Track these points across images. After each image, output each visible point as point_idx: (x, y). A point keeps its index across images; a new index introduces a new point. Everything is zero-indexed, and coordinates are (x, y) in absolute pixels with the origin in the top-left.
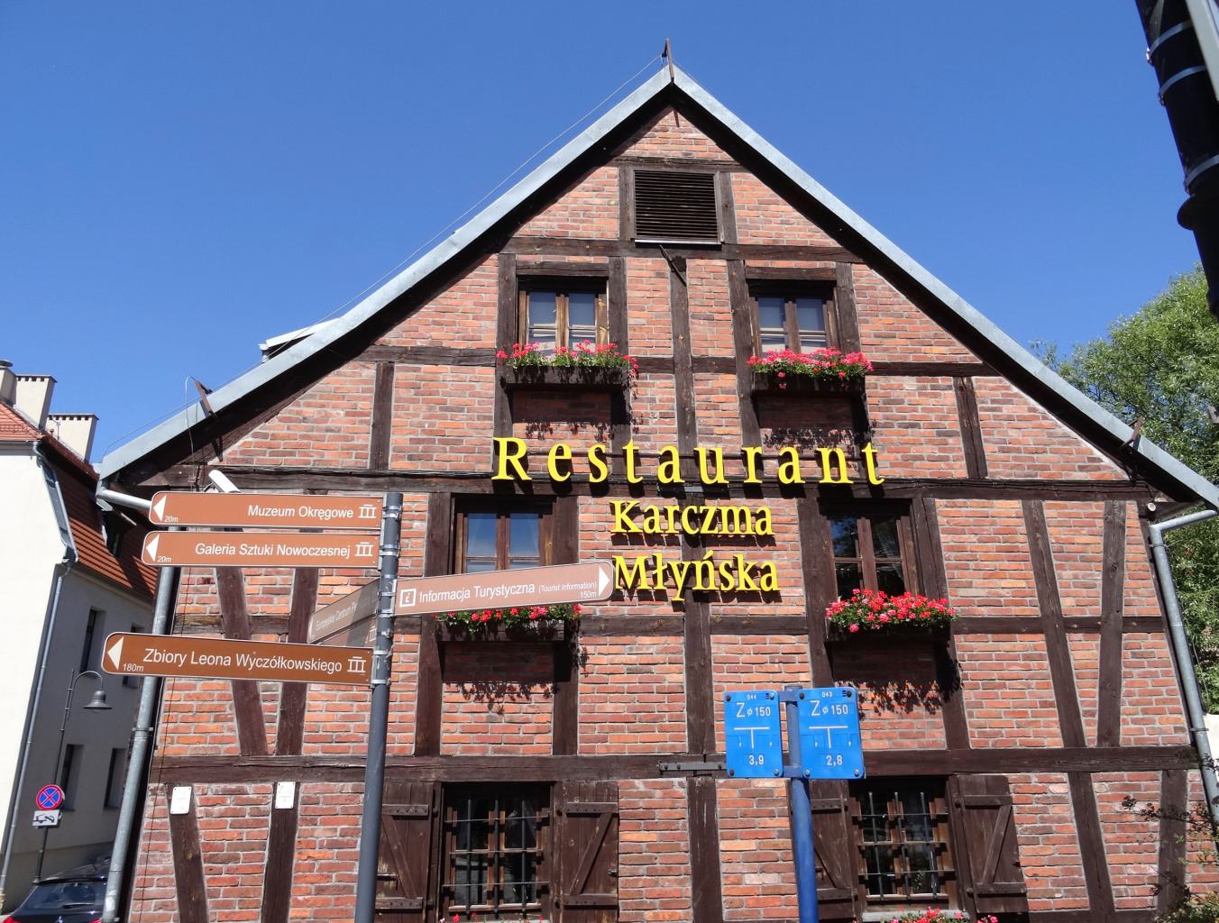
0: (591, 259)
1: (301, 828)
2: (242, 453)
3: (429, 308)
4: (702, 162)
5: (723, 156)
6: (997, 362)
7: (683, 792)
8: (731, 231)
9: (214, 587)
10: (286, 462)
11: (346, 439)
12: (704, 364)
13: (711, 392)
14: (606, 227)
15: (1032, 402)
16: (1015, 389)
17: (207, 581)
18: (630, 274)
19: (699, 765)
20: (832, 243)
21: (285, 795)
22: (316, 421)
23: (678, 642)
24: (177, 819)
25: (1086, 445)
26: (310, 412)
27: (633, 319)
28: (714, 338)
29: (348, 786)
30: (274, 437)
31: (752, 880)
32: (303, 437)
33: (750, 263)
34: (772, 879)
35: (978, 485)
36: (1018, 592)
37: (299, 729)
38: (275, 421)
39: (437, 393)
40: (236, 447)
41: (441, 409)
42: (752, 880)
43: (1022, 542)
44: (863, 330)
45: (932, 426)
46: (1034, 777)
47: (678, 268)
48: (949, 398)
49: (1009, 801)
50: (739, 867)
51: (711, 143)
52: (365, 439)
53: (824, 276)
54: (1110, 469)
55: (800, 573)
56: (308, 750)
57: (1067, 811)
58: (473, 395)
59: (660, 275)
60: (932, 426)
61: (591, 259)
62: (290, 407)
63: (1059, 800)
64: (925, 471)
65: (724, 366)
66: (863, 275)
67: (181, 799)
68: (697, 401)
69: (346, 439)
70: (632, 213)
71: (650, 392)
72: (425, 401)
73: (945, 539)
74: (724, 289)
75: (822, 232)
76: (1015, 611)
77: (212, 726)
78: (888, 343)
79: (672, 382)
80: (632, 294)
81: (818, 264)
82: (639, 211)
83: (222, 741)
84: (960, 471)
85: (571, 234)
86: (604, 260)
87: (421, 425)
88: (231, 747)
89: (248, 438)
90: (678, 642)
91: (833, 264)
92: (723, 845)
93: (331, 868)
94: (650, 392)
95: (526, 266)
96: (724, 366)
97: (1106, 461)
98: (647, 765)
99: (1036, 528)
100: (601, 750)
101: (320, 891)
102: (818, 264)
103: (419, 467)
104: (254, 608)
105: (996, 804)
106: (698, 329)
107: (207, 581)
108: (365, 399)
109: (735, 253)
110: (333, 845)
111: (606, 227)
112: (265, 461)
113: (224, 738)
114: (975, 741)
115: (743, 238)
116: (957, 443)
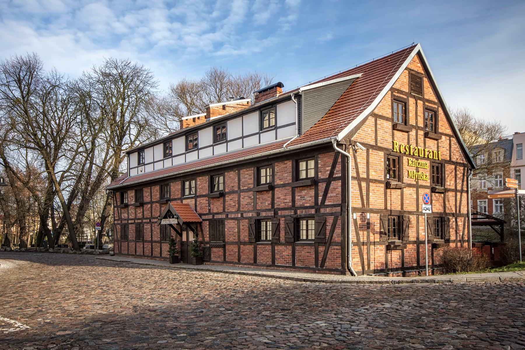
2: (356, 137)
10: (362, 141)
13: (420, 135)
17: (354, 169)
19: (417, 213)
20: (436, 101)
22: (367, 131)
30: (361, 134)
32: (365, 135)
35: (450, 162)
38: (360, 130)
39: (383, 127)
41: (385, 132)
45: (446, 148)
47: (416, 103)
56: (371, 207)
58: (389, 129)
60: (446, 148)
66: (440, 111)
72: (382, 129)
83: (359, 204)
86: (405, 97)
87: (382, 135)
104: (361, 176)
106: (419, 118)
107: (354, 169)
108: (373, 127)
109: (423, 100)
115: (426, 97)
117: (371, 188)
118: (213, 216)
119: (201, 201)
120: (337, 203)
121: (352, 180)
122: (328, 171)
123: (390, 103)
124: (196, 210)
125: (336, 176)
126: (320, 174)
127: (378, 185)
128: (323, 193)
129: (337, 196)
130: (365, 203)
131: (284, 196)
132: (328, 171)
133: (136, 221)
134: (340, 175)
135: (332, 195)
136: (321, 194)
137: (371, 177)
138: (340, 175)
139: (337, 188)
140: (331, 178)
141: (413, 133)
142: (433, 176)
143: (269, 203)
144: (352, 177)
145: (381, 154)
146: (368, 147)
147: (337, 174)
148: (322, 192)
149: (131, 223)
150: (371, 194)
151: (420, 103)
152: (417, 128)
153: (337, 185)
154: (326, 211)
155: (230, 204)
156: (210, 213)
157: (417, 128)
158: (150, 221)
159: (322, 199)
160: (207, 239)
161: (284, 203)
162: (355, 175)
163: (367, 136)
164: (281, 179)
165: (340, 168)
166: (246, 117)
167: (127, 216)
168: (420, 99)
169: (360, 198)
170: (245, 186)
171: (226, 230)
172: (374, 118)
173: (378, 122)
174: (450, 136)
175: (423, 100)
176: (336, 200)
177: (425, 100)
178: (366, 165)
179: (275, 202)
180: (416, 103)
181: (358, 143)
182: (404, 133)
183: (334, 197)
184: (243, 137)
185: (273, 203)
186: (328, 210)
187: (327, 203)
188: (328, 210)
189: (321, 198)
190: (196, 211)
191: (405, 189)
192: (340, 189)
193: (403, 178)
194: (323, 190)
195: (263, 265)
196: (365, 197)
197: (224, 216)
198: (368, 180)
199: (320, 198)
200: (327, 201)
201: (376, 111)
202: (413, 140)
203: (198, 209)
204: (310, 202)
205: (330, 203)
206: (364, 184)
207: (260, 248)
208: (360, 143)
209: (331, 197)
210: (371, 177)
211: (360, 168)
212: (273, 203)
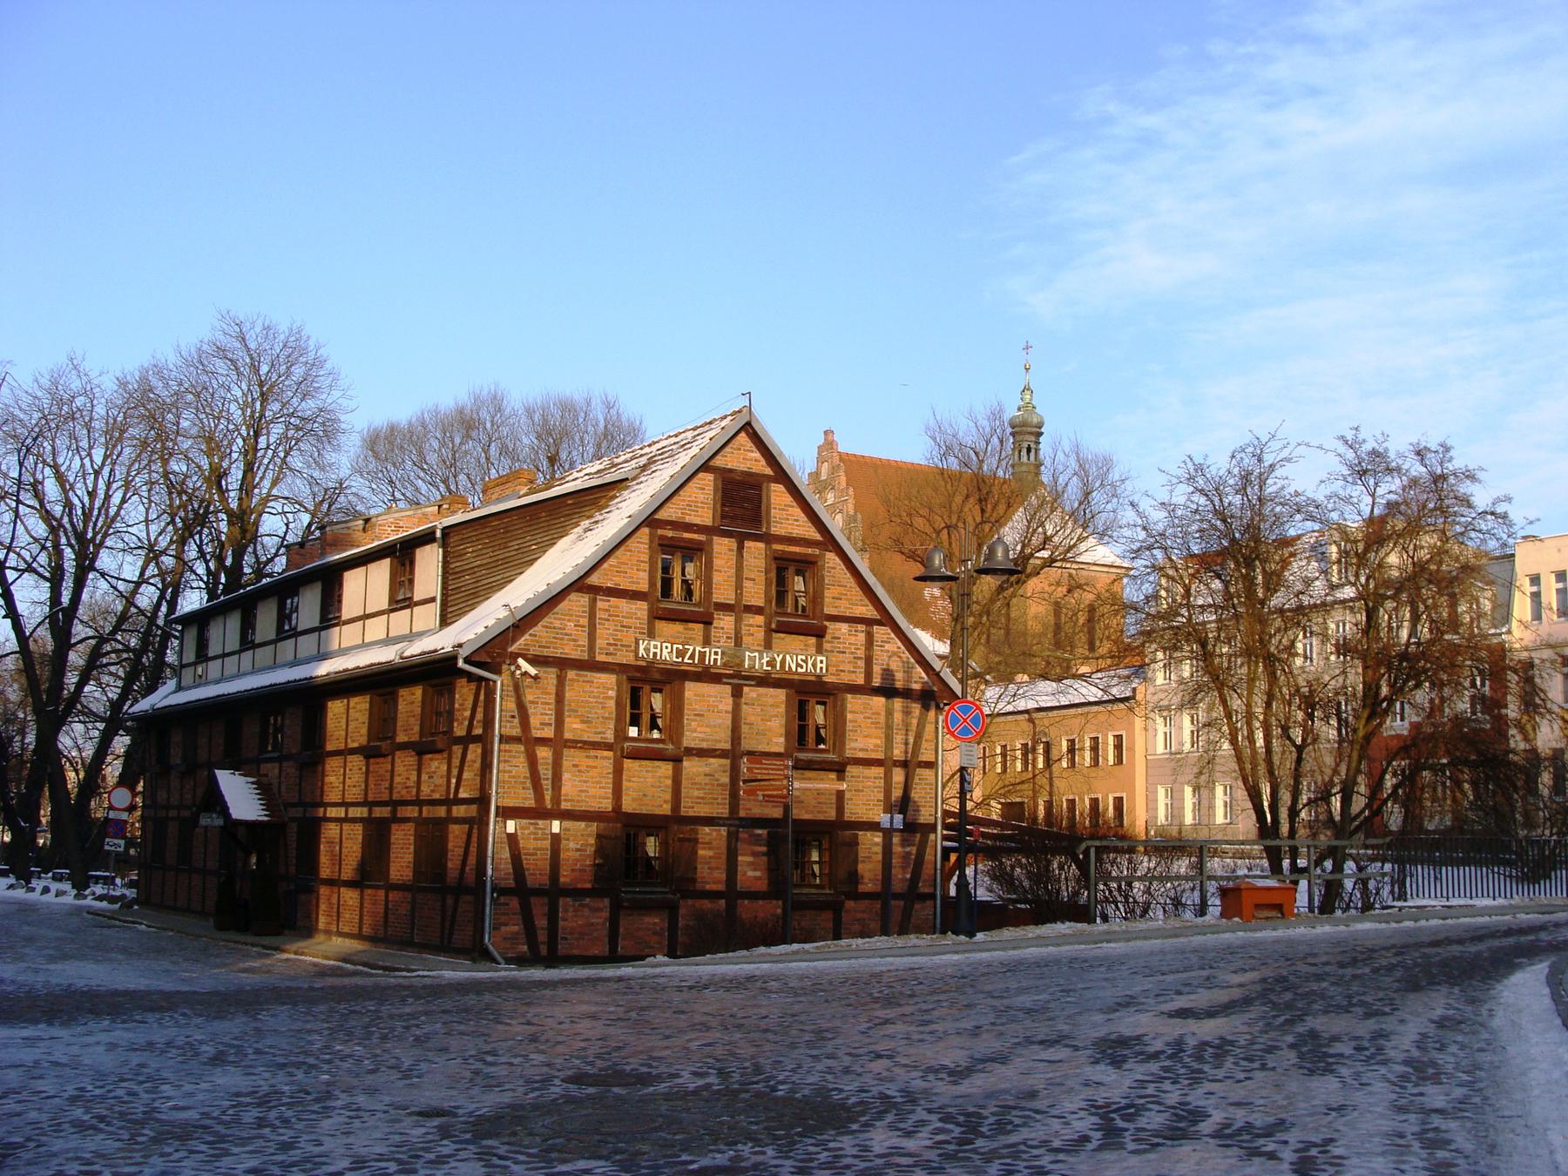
0: (695, 536)
1: (564, 842)
3: (612, 561)
4: (758, 475)
5: (768, 471)
6: (887, 620)
7: (725, 834)
8: (768, 527)
9: (516, 720)
10: (546, 652)
11: (575, 640)
12: (749, 609)
14: (705, 517)
15: (900, 644)
16: (893, 635)
17: (513, 717)
18: (716, 548)
20: (818, 537)
21: (556, 826)
23: (727, 762)
24: (509, 835)
26: (557, 624)
27: (717, 578)
28: (755, 593)
29: (583, 824)
31: (750, 873)
33: (776, 547)
34: (758, 874)
36: (876, 746)
37: (560, 795)
40: (522, 641)
42: (750, 873)
43: (882, 719)
44: (827, 593)
46: (869, 834)
47: (741, 548)
48: (862, 637)
49: (857, 844)
50: (745, 868)
51: (763, 462)
52: (584, 641)
53: (811, 559)
55: (783, 731)
57: (879, 849)
59: (730, 550)
61: (695, 536)
62: (546, 619)
63: (877, 844)
64: (846, 678)
65: (758, 610)
66: (831, 558)
67: (511, 826)
68: (744, 630)
69: (575, 640)
70: (719, 506)
71: (722, 624)
73: (849, 716)
74: (761, 563)
75: (813, 529)
76: (874, 756)
77: (521, 791)
78: (838, 603)
79: (733, 619)
80: (718, 562)
81: (810, 551)
82: (723, 505)
83: (525, 799)
84: (860, 680)
85: (688, 519)
86: (702, 538)
88: (530, 803)
89: (527, 636)
90: (727, 762)
91: (817, 552)
92: (740, 858)
93: (577, 860)
94: (722, 624)
95: (662, 537)
96: (758, 610)
98: (710, 821)
99: (889, 713)
100: (691, 813)
101: (573, 870)
102: (810, 551)
103: (610, 659)
104: (537, 734)
105: (854, 843)
106: (747, 584)
107: (513, 717)
109: (768, 539)
110: (578, 850)
111: (705, 517)
112: (534, 651)
113: (526, 799)
114: (848, 816)
115: (776, 530)
116: (861, 663)
117: (566, 764)
121: (501, 742)
123: (646, 558)
124: (279, 792)
126: (455, 724)
127: (592, 753)
130: (548, 797)
136: (455, 772)
137: (568, 735)
140: (469, 739)
141: (725, 622)
144: (501, 737)
145: (609, 680)
146: (563, 664)
149: (173, 819)
150: (566, 776)
152: (738, 609)
153: (475, 751)
156: (301, 804)
157: (738, 609)
160: (293, 869)
162: (516, 731)
163: (562, 639)
166: (373, 567)
168: (757, 538)
169: (529, 784)
172: (587, 596)
173: (600, 604)
174: (869, 622)
175: (768, 539)
178: (553, 707)
180: (741, 548)
181: (521, 661)
182: (691, 625)
184: (366, 617)
191: (686, 763)
193: (682, 734)
196: (547, 784)
198: (559, 743)
200: (461, 790)
201: (594, 580)
203: (283, 789)
206: (544, 753)
210: (568, 735)
211: (535, 714)
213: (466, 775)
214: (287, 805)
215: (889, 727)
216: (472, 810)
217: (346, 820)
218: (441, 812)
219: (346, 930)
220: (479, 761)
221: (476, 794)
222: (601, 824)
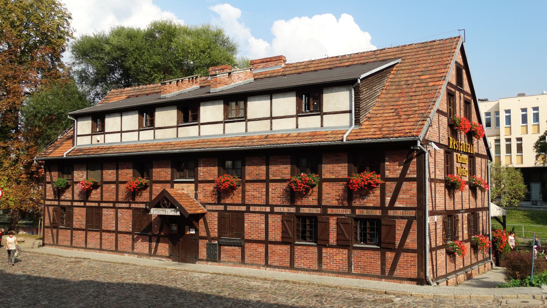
20: (469, 92)
25: (484, 147)
51: (462, 60)
54: (485, 153)
97: (486, 151)
116: (477, 144)
118: (225, 208)
119: (205, 188)
120: (412, 206)
122: (398, 169)
125: (410, 176)
128: (392, 194)
129: (412, 199)
131: (336, 192)
132: (398, 169)
133: (88, 204)
134: (415, 176)
135: (404, 196)
138: (415, 176)
139: (411, 190)
140: (402, 179)
142: (470, 170)
143: (314, 198)
147: (411, 174)
148: (390, 192)
150: (437, 194)
151: (462, 95)
154: (396, 213)
155: (254, 195)
158: (114, 205)
159: (391, 200)
160: (214, 233)
161: (335, 200)
164: (332, 173)
165: (416, 168)
167: (71, 196)
170: (277, 176)
171: (246, 225)
176: (410, 203)
177: (465, 93)
179: (323, 198)
183: (408, 199)
184: (271, 118)
185: (320, 199)
186: (399, 213)
187: (397, 205)
188: (399, 213)
189: (389, 198)
190: (197, 200)
192: (415, 191)
194: (393, 190)
195: (329, 272)
197: (244, 208)
199: (388, 199)
202: (436, 128)
204: (375, 202)
205: (401, 206)
207: (298, 249)
208: (435, 143)
209: (403, 199)
212: (320, 199)
213: (400, 196)
214: (204, 204)
215: (481, 170)
216: (412, 213)
217: (272, 212)
218: (378, 213)
219: (275, 264)
220: (415, 190)
221: (416, 206)
222: (444, 216)
